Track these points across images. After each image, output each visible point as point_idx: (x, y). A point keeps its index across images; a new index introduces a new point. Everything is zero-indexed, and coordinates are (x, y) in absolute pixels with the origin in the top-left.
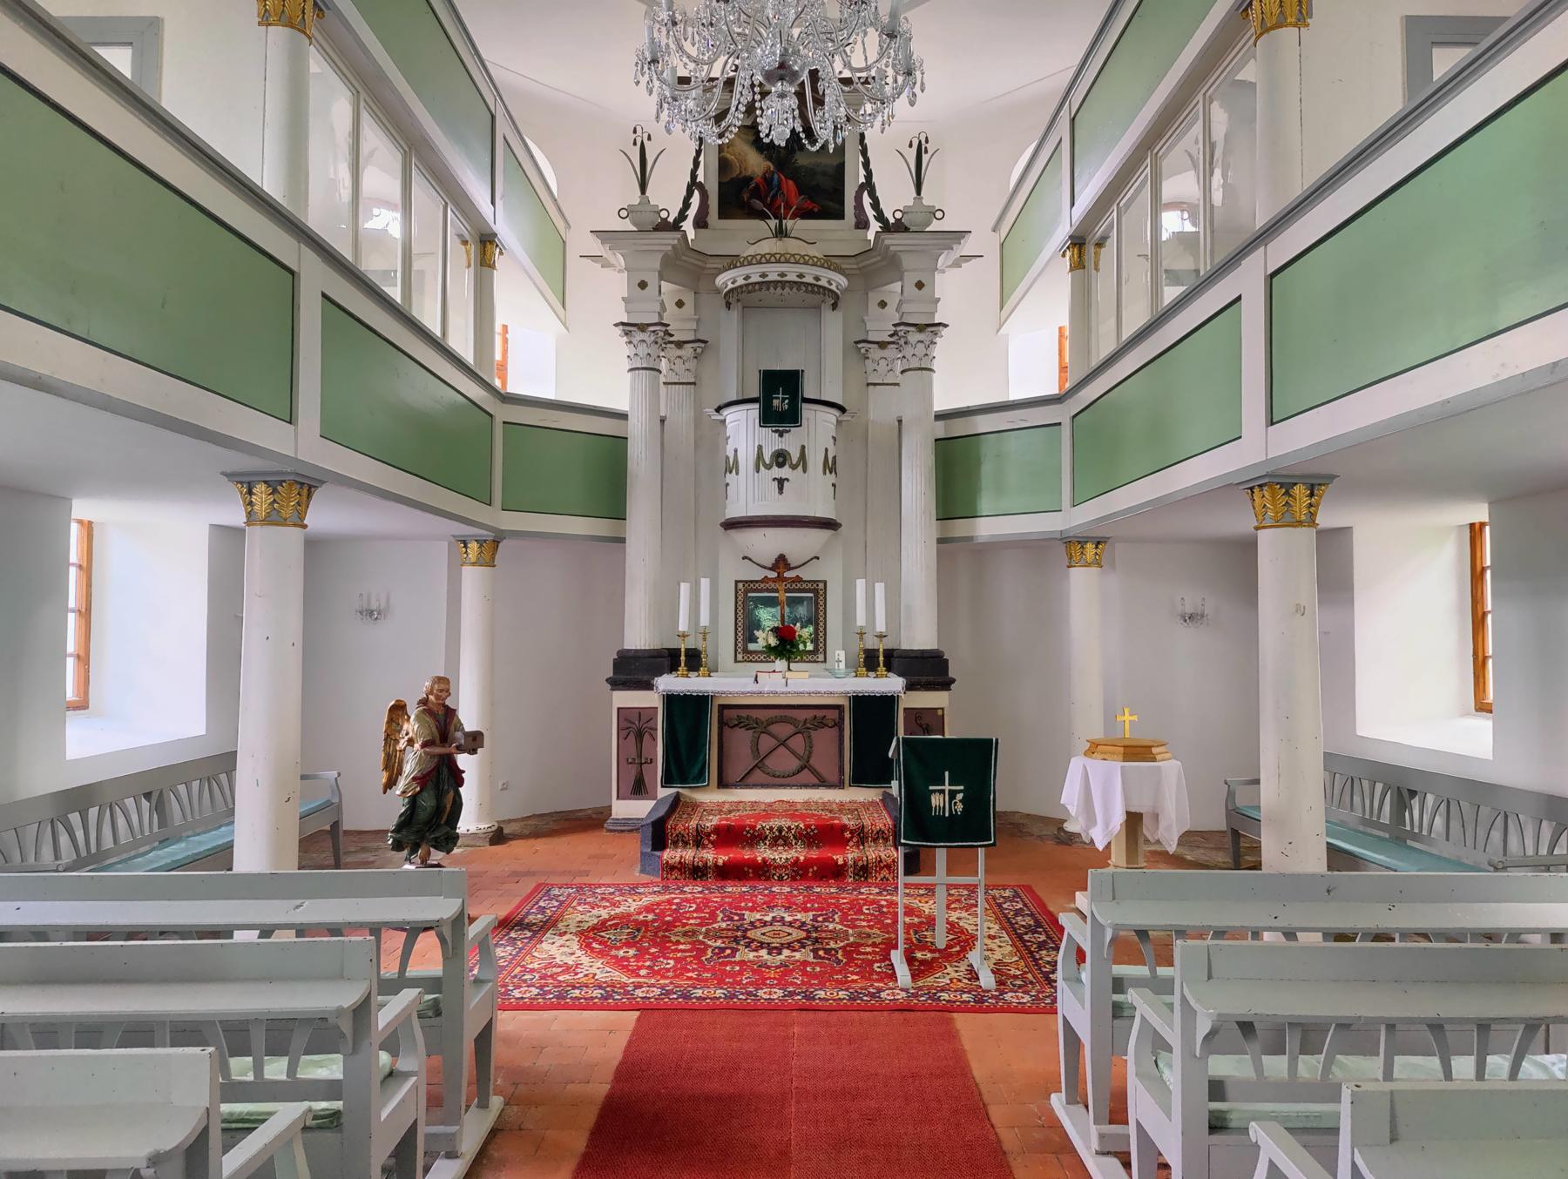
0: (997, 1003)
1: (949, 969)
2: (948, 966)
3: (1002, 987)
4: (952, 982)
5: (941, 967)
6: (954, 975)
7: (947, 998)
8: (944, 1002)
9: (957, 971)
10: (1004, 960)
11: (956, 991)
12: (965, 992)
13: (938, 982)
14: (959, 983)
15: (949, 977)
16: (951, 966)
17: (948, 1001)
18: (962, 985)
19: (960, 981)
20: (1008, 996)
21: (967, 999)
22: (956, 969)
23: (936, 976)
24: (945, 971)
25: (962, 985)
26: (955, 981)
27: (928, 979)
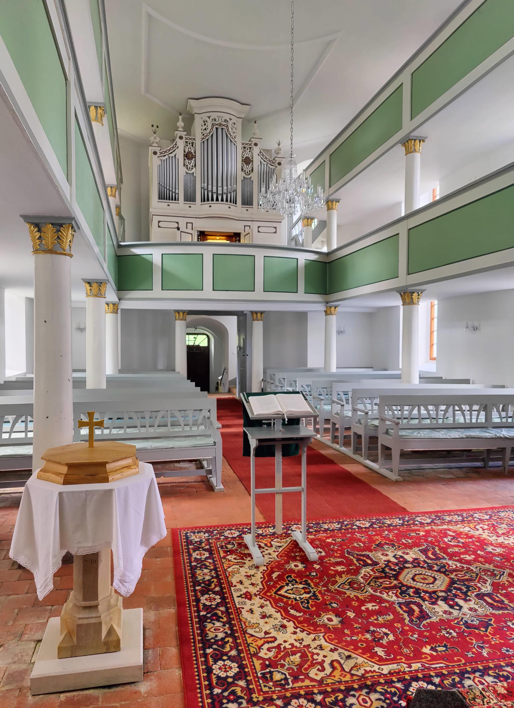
0: (243, 529)
1: (275, 555)
2: (276, 558)
3: (240, 541)
4: (270, 543)
5: (281, 556)
6: (271, 550)
7: (270, 529)
8: (270, 525)
9: (270, 554)
10: (238, 566)
11: (266, 535)
12: (261, 535)
13: (278, 542)
14: (266, 542)
15: (273, 549)
16: (274, 558)
17: (268, 527)
18: (264, 542)
19: (266, 545)
20: (237, 534)
21: (259, 530)
22: (271, 556)
23: (281, 549)
24: (277, 553)
25: (264, 542)
26: (269, 545)
27: (286, 545)
